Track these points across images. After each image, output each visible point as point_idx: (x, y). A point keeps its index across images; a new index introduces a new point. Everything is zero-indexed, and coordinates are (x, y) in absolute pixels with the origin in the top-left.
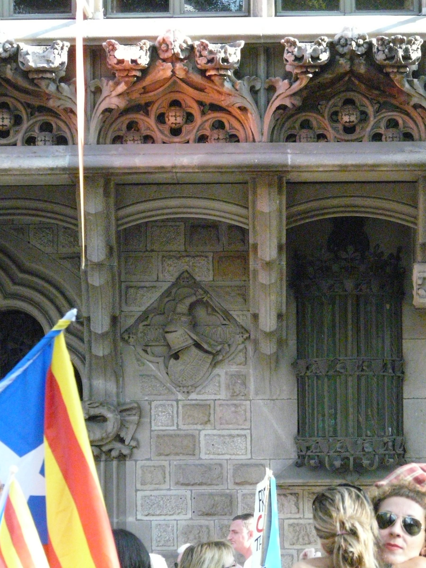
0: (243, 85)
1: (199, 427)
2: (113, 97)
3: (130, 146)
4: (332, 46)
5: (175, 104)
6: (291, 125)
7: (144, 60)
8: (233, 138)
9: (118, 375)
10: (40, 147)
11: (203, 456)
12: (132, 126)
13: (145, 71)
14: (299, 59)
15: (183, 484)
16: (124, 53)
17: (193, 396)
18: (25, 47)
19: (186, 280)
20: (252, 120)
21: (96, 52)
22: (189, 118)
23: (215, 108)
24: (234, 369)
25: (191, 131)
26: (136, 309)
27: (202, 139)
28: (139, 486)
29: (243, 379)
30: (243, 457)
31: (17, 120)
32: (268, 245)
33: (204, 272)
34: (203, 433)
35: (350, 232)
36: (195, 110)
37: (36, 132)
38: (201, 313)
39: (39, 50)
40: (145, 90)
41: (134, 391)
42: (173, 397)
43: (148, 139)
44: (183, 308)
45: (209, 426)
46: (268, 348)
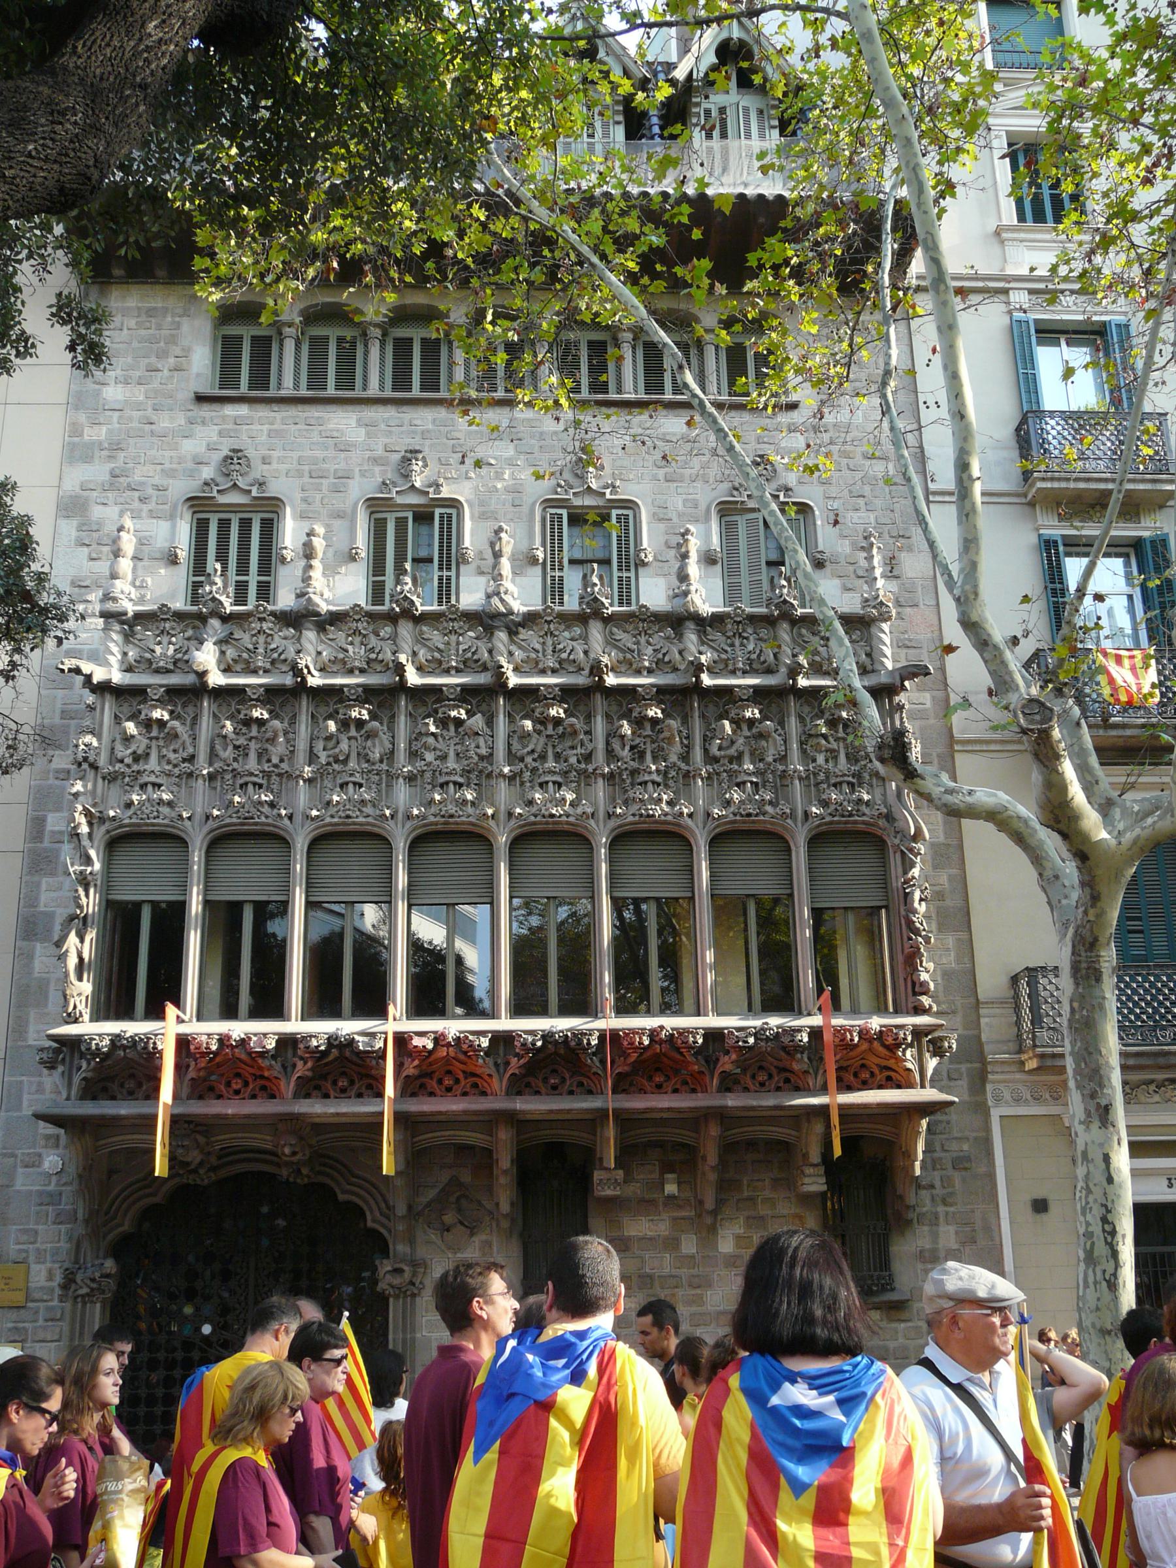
0: (490, 1061)
2: (411, 1069)
3: (421, 1098)
4: (543, 1037)
5: (449, 1072)
6: (519, 1086)
7: (430, 1046)
8: (484, 1093)
9: (412, 1242)
10: (366, 1100)
12: (422, 1086)
13: (430, 1052)
14: (524, 1045)
16: (417, 1042)
18: (357, 1038)
19: (455, 1182)
20: (496, 1083)
21: (401, 1040)
22: (457, 1081)
23: (474, 1075)
24: (484, 1237)
25: (458, 1090)
26: (424, 1200)
27: (465, 1094)
29: (489, 1244)
31: (352, 1083)
32: (505, 1160)
33: (466, 1177)
35: (555, 1151)
36: (461, 1076)
37: (363, 1090)
38: (463, 1202)
39: (366, 1039)
40: (431, 1064)
41: (422, 1252)
43: (432, 1094)
44: (453, 1199)
46: (505, 1224)
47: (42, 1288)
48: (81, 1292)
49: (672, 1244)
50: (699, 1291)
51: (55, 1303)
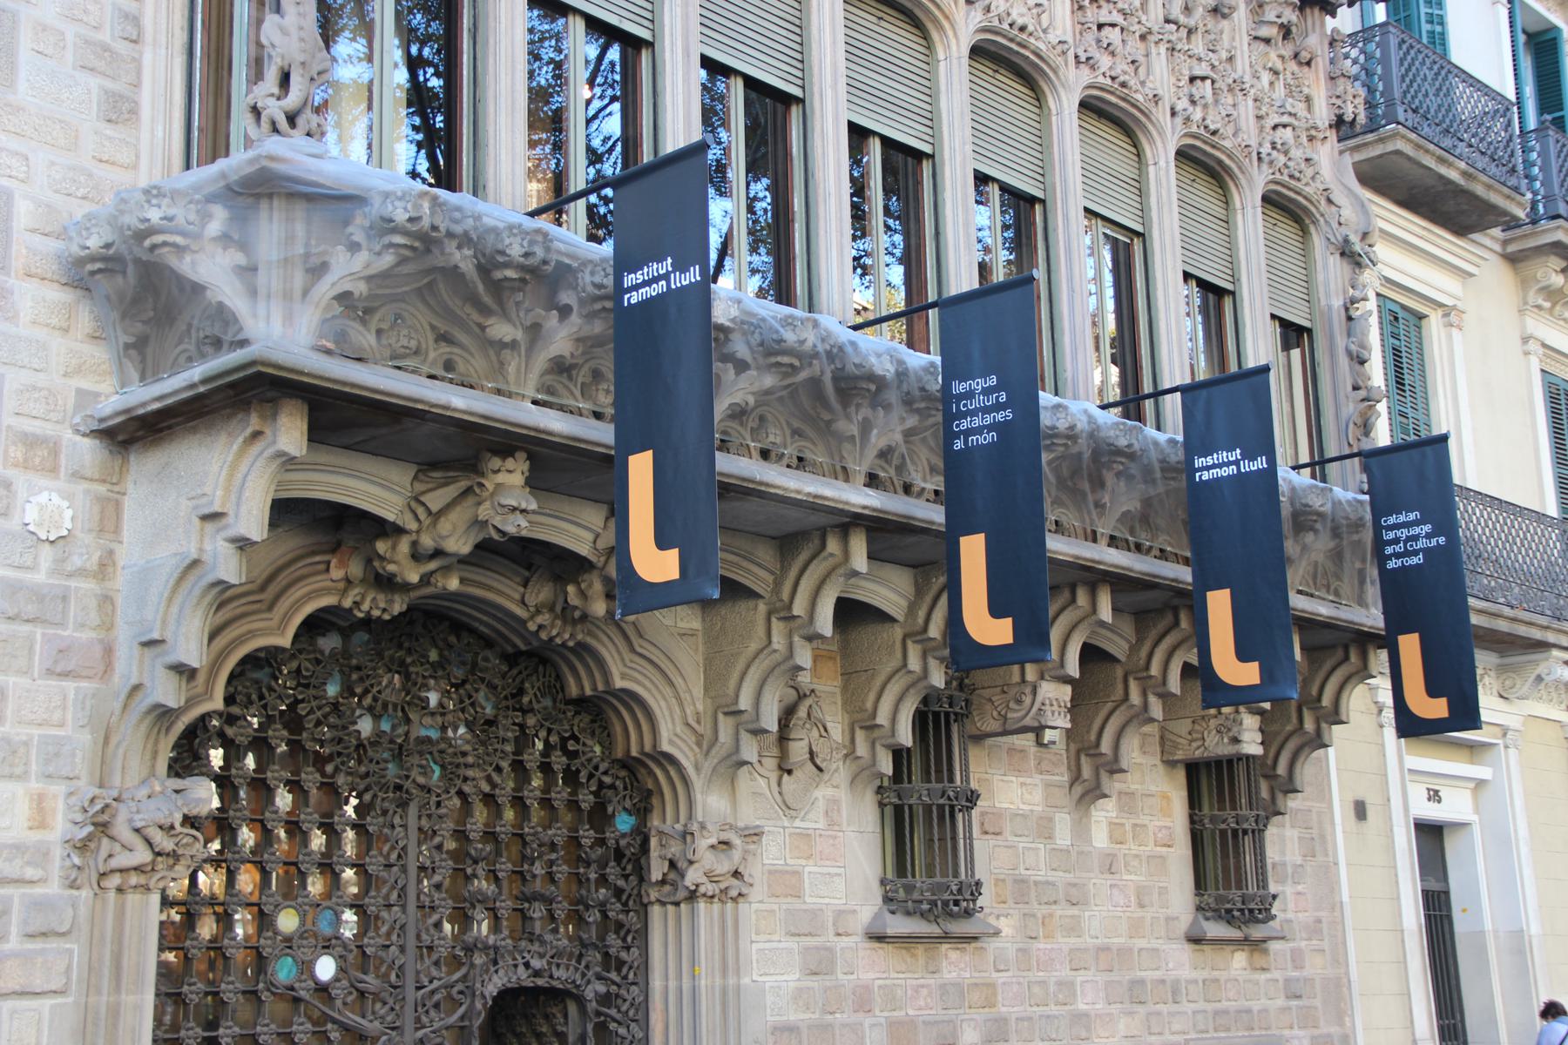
1: (803, 862)
11: (808, 900)
15: (793, 935)
17: (797, 823)
28: (754, 937)
30: (839, 902)
34: (807, 869)
42: (779, 823)
45: (811, 862)
47: (18, 848)
48: (123, 860)
49: (1045, 830)
50: (1074, 911)
51: (54, 888)
